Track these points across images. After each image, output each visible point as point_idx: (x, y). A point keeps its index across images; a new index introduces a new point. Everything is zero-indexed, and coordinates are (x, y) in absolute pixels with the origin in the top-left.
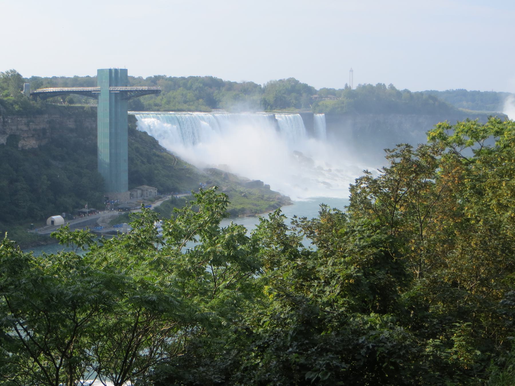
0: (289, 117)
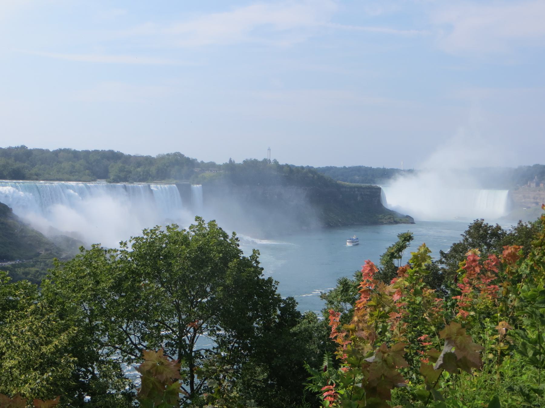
0: (165, 188)
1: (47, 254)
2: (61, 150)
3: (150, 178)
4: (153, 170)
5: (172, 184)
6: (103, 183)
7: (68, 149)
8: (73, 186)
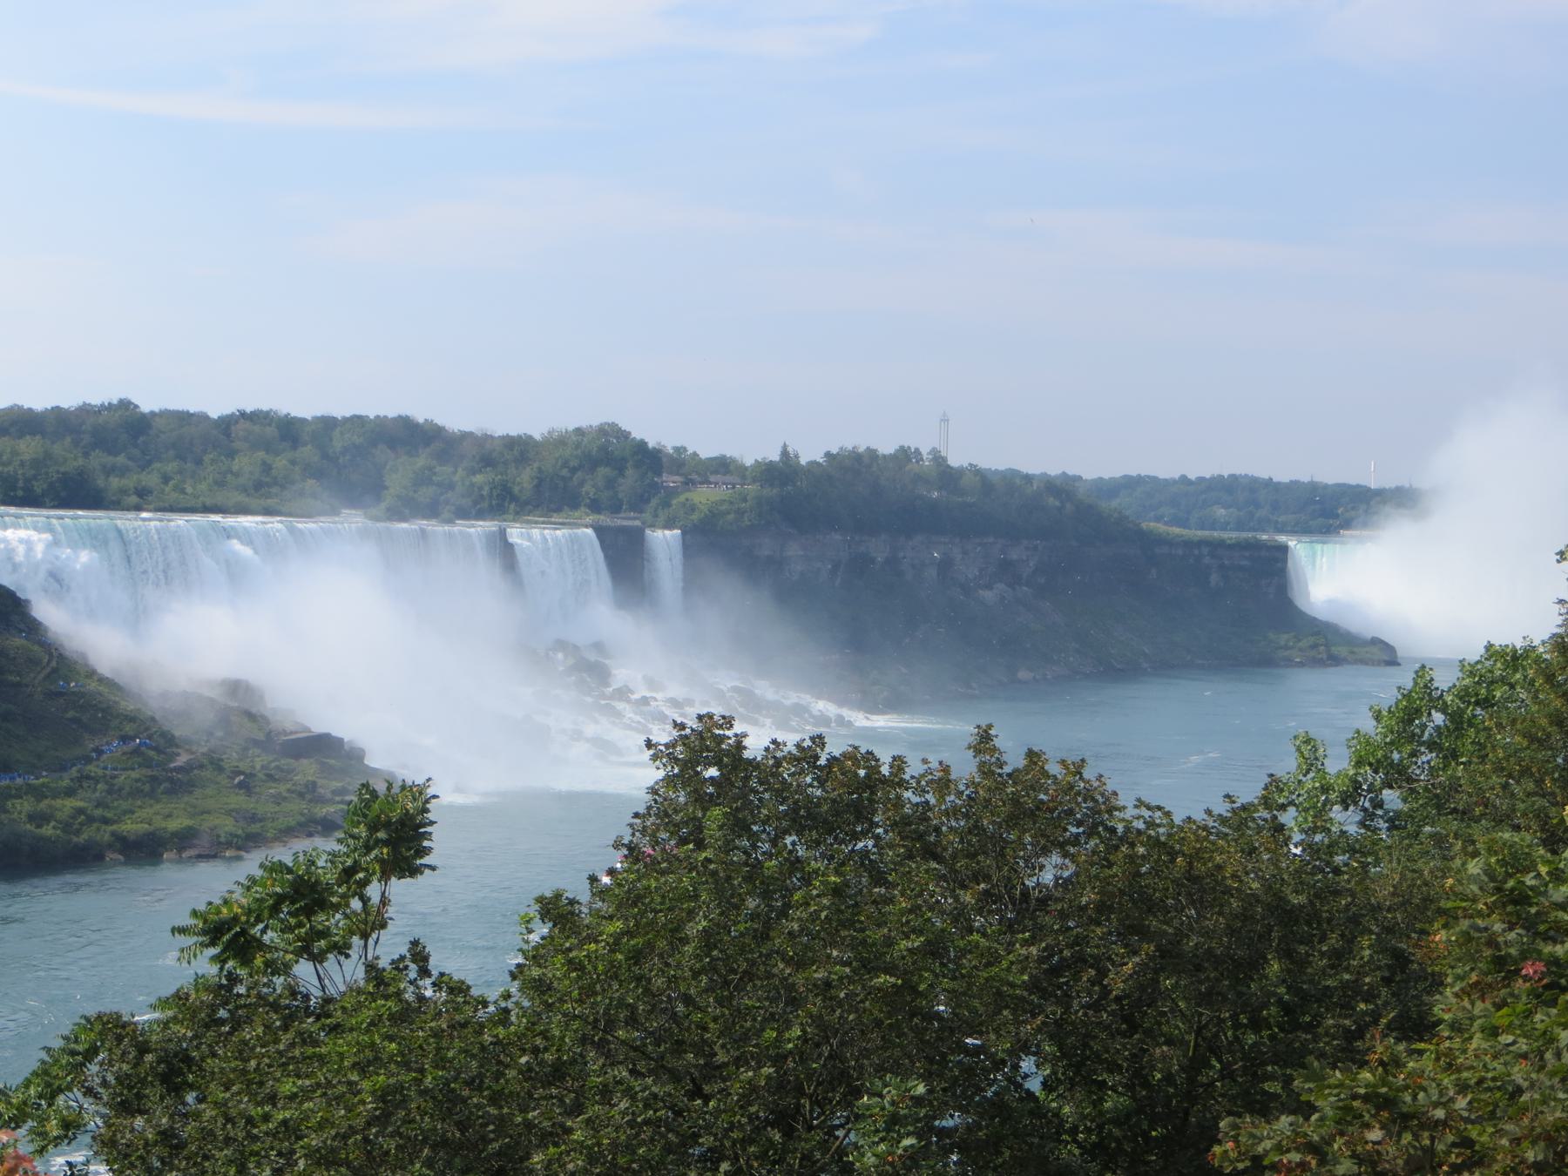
0: (556, 539)
1: (124, 754)
2: (243, 414)
3: (512, 506)
4: (524, 480)
5: (578, 526)
7: (268, 413)
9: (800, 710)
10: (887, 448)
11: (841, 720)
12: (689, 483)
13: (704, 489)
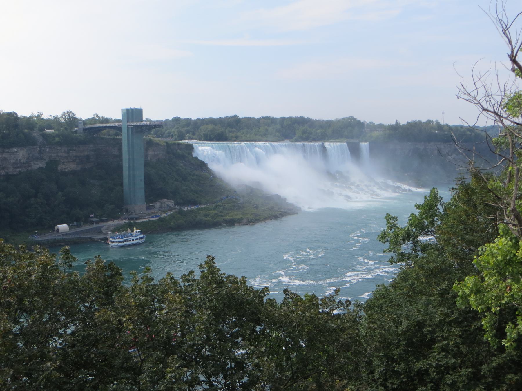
6: (287, 142)
8: (260, 145)
9: (398, 187)
10: (424, 120)
11: (409, 190)
12: (371, 131)
13: (375, 132)
